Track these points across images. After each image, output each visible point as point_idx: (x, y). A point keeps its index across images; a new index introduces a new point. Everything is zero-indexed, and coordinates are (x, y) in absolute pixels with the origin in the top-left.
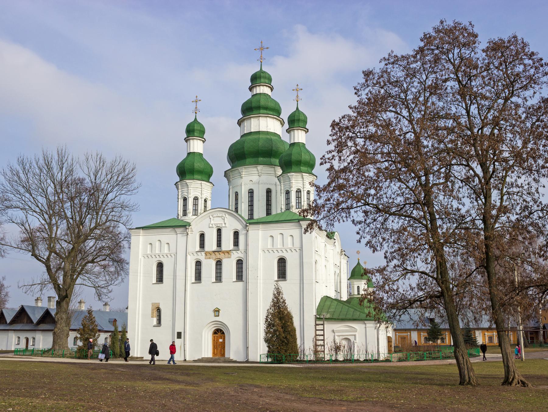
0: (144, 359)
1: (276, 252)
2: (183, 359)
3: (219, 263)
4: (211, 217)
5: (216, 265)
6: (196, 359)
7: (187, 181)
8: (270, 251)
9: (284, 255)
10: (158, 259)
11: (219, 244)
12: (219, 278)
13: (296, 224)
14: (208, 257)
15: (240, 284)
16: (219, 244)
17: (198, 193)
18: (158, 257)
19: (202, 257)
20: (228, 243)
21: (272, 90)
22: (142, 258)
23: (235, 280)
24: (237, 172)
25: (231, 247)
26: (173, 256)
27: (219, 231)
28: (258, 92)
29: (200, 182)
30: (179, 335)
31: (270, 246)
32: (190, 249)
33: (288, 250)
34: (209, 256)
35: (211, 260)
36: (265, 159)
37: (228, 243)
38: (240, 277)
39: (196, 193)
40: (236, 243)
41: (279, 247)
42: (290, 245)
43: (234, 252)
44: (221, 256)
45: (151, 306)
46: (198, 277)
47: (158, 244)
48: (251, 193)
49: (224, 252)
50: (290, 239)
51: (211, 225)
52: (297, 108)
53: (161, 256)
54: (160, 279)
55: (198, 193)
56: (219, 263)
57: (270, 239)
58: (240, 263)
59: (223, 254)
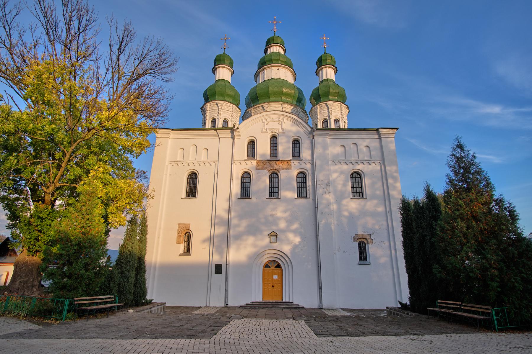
3: (274, 176)
7: (218, 102)
12: (274, 193)
17: (228, 116)
18: (191, 165)
19: (251, 165)
22: (170, 166)
26: (213, 165)
28: (275, 51)
29: (231, 105)
32: (236, 157)
35: (265, 171)
39: (226, 115)
41: (353, 159)
45: (177, 227)
47: (192, 149)
49: (282, 162)
51: (264, 130)
53: (197, 165)
54: (192, 192)
55: (228, 116)
56: (274, 176)
58: (302, 175)
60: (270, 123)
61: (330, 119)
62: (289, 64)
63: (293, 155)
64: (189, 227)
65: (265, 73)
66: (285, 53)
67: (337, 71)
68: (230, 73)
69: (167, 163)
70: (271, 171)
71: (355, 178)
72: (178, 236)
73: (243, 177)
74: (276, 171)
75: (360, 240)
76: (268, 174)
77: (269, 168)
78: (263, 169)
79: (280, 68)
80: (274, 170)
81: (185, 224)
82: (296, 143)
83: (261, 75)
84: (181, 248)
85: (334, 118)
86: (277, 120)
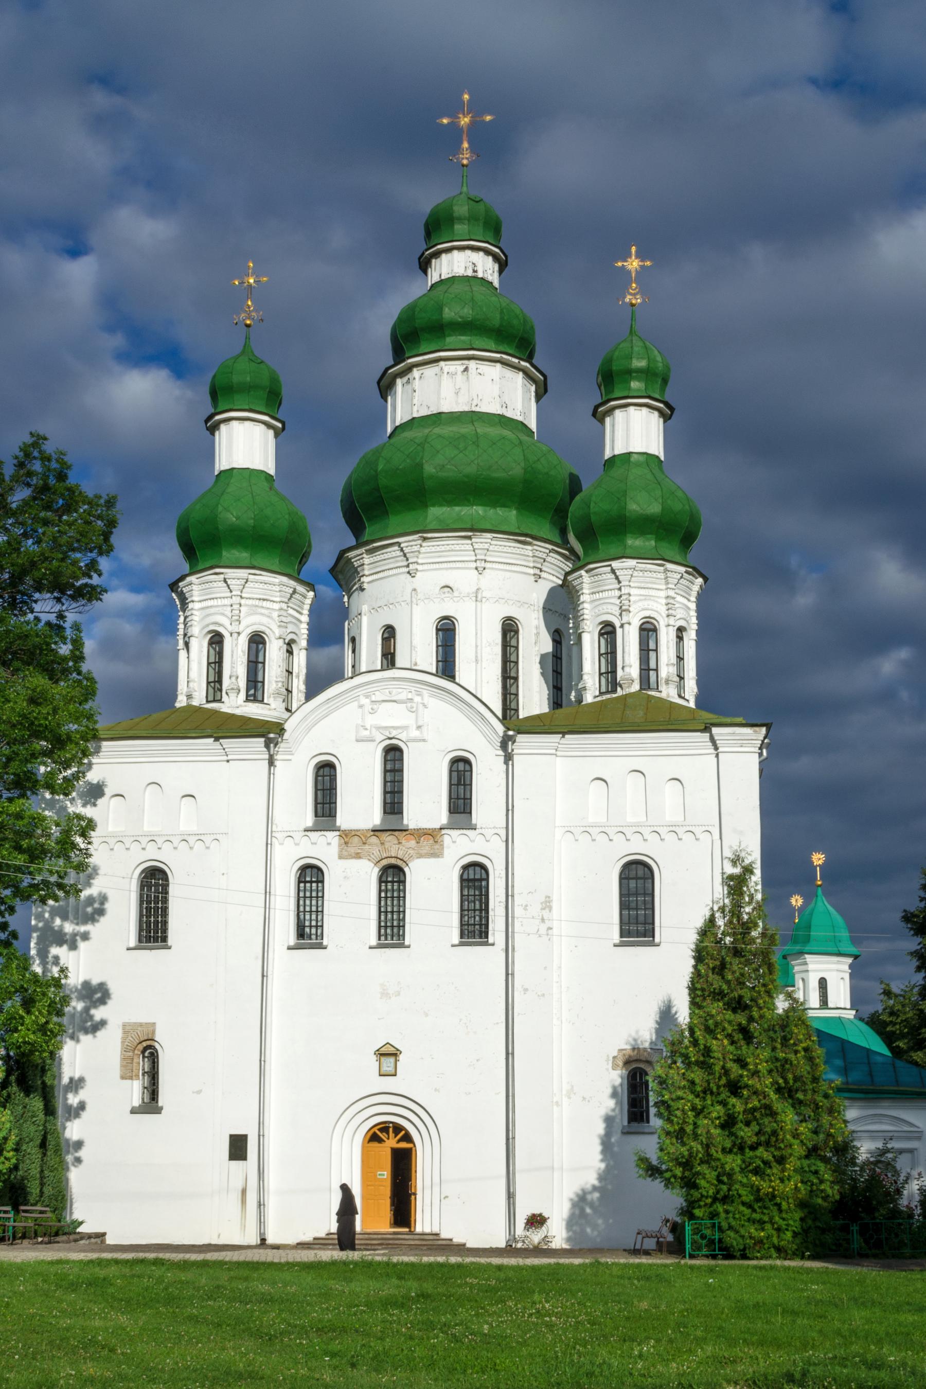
0: (110, 1241)
2: (254, 1240)
3: (393, 877)
4: (364, 701)
5: (381, 881)
6: (308, 1237)
7: (230, 573)
11: (393, 802)
12: (392, 929)
14: (352, 850)
16: (393, 802)
17: (265, 620)
19: (324, 849)
20: (426, 802)
21: (501, 272)
23: (456, 939)
24: (394, 551)
25: (440, 815)
27: (393, 755)
30: (238, 1147)
36: (491, 512)
37: (426, 802)
38: (474, 928)
40: (460, 804)
41: (630, 819)
48: (446, 631)
55: (265, 620)
56: (393, 877)
59: (413, 843)
61: (622, 626)
62: (513, 340)
64: (154, 1032)
65: (417, 384)
66: (503, 265)
68: (271, 433)
70: (385, 862)
71: (637, 878)
72: (124, 1059)
73: (301, 880)
74: (400, 863)
75: (634, 1066)
76: (375, 872)
77: (376, 852)
78: (358, 856)
79: (472, 364)
80: (393, 861)
81: (141, 1025)
82: (461, 771)
84: (135, 1091)
85: (636, 623)
86: (403, 696)
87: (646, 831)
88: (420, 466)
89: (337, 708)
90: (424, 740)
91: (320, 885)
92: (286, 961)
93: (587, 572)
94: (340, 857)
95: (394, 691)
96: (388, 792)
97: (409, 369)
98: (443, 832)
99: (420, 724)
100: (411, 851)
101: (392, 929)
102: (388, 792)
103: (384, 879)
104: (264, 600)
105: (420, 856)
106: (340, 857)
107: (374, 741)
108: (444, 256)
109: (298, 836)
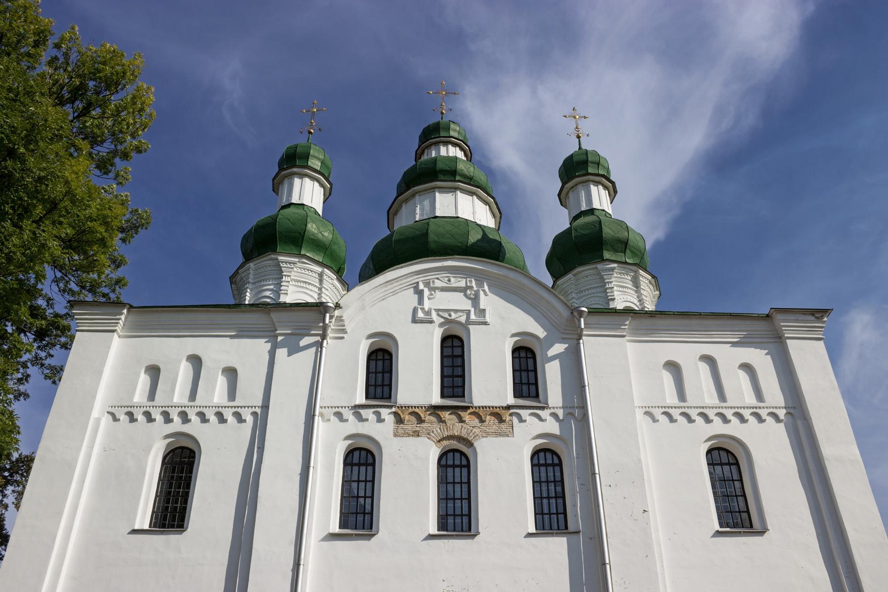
1: (700, 420)
7: (281, 258)
8: (675, 413)
9: (734, 429)
10: (178, 425)
12: (457, 514)
13: (761, 326)
15: (558, 545)
22: (106, 420)
26: (250, 419)
31: (671, 398)
33: (746, 413)
34: (410, 423)
35: (423, 440)
42: (750, 399)
43: (524, 413)
44: (469, 426)
46: (359, 514)
47: (185, 370)
50: (743, 377)
52: (580, 148)
54: (172, 512)
57: (667, 378)
60: (438, 294)
63: (518, 394)
67: (615, 192)
69: (98, 410)
76: (434, 452)
78: (417, 434)
83: (405, 209)
86: (462, 283)
87: (729, 414)
88: (426, 234)
89: (394, 293)
90: (485, 323)
91: (370, 468)
92: (325, 556)
93: (574, 275)
94: (395, 435)
95: (452, 280)
96: (448, 376)
97: (413, 196)
98: (512, 411)
99: (482, 307)
100: (476, 430)
101: (457, 514)
102: (448, 376)
103: (443, 462)
104: (309, 284)
105: (487, 434)
106: (395, 435)
107: (431, 322)
108: (433, 147)
109: (348, 414)
